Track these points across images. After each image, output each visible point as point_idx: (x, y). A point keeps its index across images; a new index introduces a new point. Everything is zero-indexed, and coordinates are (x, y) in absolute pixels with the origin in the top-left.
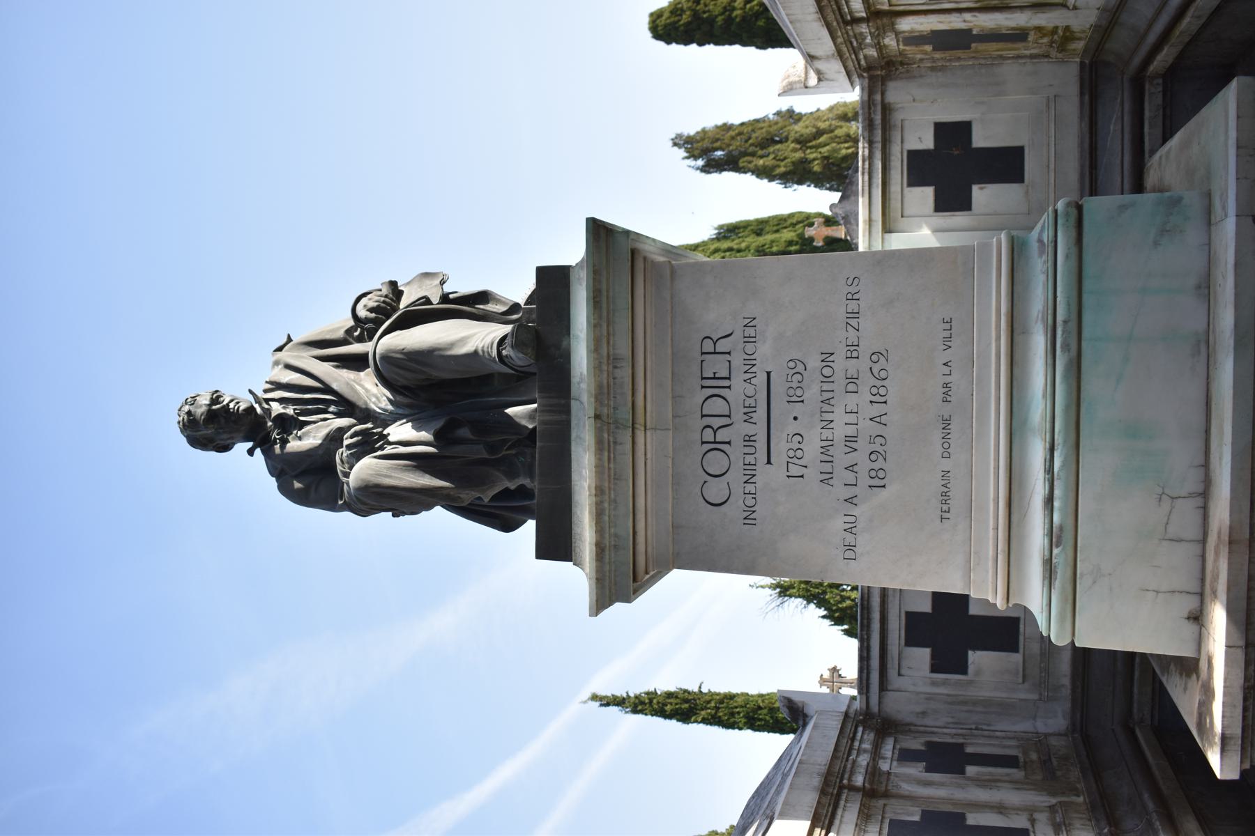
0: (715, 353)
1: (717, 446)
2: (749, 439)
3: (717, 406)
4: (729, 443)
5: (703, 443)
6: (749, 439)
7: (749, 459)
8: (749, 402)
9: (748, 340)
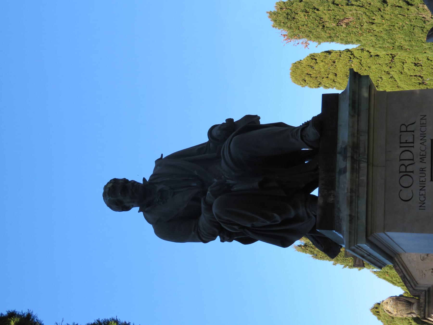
0: (407, 131)
1: (407, 173)
2: (422, 170)
3: (407, 155)
4: (413, 172)
5: (400, 172)
6: (422, 170)
7: (422, 179)
8: (423, 153)
9: (423, 125)
